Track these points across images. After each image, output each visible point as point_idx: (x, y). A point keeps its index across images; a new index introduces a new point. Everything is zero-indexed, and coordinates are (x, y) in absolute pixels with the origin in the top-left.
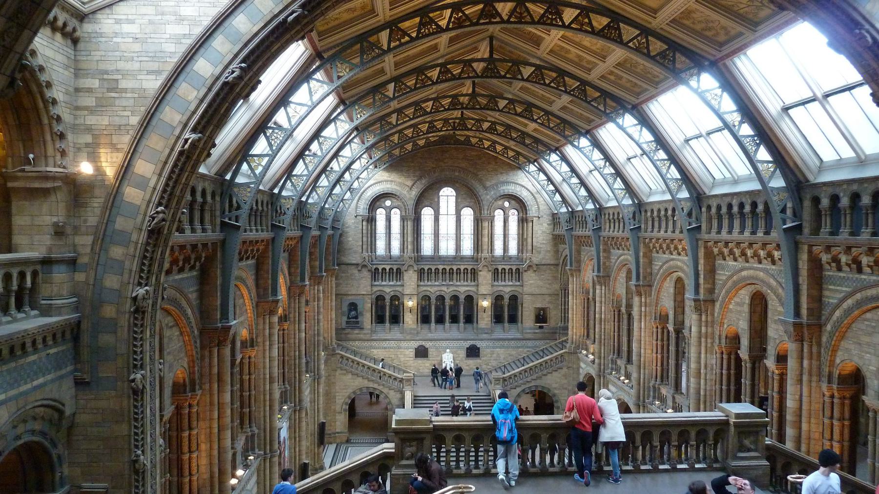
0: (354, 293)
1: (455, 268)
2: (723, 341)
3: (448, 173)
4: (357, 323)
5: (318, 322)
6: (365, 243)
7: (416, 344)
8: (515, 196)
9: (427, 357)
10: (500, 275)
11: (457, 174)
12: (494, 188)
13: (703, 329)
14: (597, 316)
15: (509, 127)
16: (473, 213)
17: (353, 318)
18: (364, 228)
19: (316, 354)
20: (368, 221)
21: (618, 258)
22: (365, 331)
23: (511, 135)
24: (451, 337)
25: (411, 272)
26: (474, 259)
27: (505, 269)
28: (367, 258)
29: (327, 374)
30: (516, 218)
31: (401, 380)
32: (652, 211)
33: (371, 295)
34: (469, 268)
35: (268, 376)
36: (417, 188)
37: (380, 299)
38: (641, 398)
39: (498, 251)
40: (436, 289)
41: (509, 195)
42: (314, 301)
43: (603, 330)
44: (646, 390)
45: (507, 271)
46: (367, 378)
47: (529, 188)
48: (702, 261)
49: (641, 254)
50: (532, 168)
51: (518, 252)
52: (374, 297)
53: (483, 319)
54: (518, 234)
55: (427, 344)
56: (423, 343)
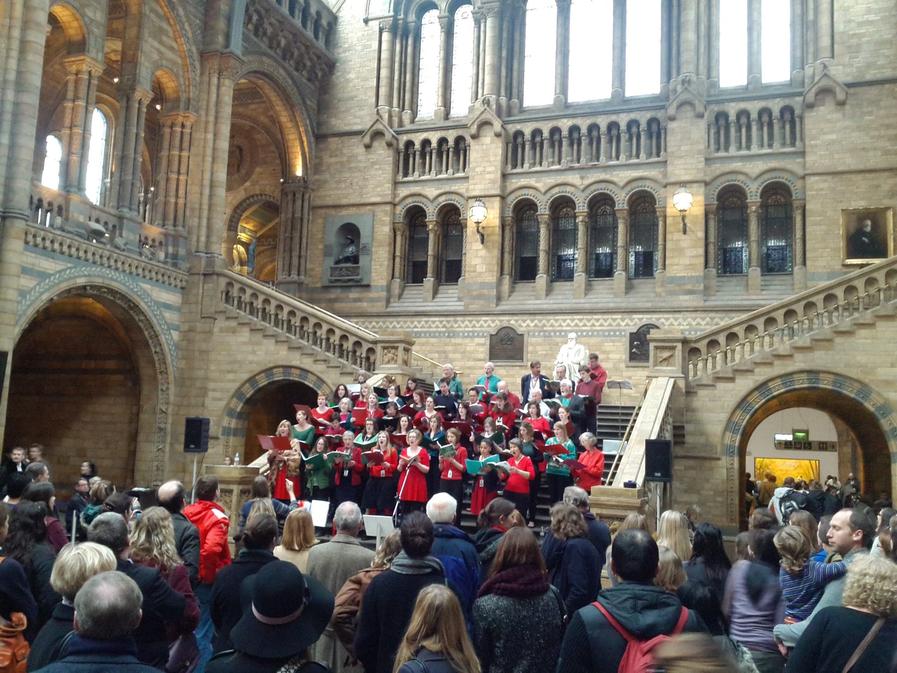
0: (352, 201)
1: (603, 122)
4: (356, 271)
5: (22, 51)
6: (384, 82)
7: (491, 325)
9: (522, 359)
10: (733, 131)
17: (347, 259)
18: (385, 46)
20: (394, 30)
22: (372, 295)
24: (587, 306)
28: (386, 116)
29: (185, 327)
34: (643, 118)
37: (415, 215)
40: (551, 180)
45: (754, 116)
46: (287, 341)
52: (400, 210)
53: (680, 251)
55: (522, 325)
56: (512, 321)
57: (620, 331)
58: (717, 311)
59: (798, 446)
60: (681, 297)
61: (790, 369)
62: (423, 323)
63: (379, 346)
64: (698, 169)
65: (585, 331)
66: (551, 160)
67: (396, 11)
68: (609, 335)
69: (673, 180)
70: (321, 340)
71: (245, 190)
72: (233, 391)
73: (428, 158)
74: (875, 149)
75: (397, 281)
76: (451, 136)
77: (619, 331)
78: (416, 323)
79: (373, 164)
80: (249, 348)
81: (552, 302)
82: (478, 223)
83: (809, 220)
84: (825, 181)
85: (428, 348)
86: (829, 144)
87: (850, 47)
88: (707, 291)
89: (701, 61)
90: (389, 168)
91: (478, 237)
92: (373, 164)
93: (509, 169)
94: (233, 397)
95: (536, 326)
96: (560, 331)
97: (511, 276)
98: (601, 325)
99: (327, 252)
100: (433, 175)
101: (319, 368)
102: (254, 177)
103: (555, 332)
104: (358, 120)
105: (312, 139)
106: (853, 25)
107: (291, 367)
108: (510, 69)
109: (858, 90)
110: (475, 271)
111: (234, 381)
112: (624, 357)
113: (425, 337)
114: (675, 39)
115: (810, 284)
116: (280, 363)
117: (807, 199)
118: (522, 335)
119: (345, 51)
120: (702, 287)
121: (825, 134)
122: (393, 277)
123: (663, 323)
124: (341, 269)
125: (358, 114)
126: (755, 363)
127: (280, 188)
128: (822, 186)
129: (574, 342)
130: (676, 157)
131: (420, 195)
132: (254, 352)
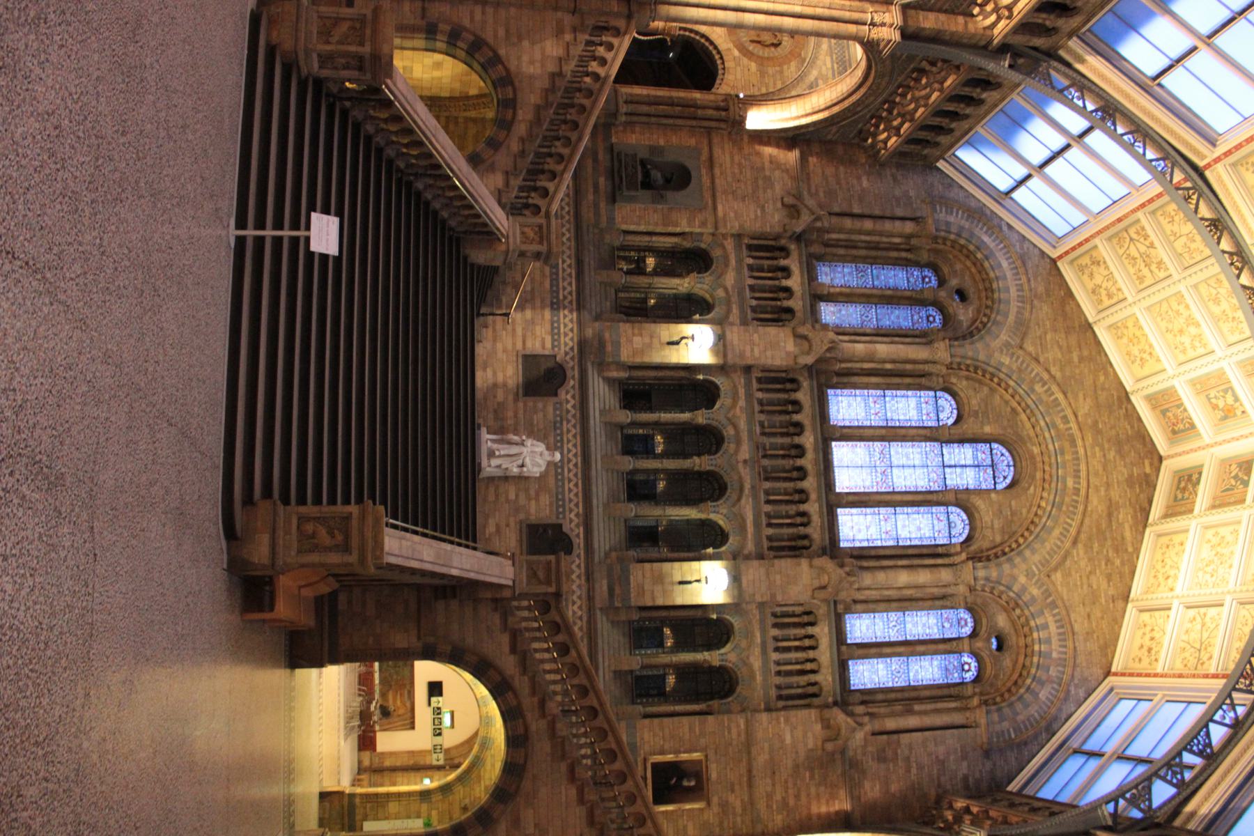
0: (717, 181)
1: (809, 484)
3: (1068, 457)
4: (632, 186)
11: (1070, 483)
12: (1047, 594)
17: (646, 174)
22: (602, 205)
24: (593, 473)
25: (790, 346)
26: (831, 547)
30: (955, 678)
36: (1020, 370)
39: (861, 628)
40: (743, 425)
55: (568, 396)
57: (564, 512)
58: (589, 622)
59: (436, 722)
60: (605, 582)
61: (529, 716)
62: (569, 270)
63: (543, 221)
64: (754, 595)
65: (563, 470)
66: (766, 424)
68: (558, 500)
69: (743, 567)
70: (550, 147)
71: (729, 49)
72: (484, 36)
73: (770, 275)
74: (774, 785)
76: (796, 303)
77: (564, 509)
78: (568, 261)
79: (763, 208)
80: (538, 56)
81: (598, 430)
82: (693, 338)
83: (696, 719)
84: (739, 735)
85: (537, 277)
86: (780, 736)
87: (884, 750)
88: (610, 609)
89: (874, 592)
90: (757, 227)
92: (763, 208)
93: (756, 374)
94: (475, 35)
95: (568, 411)
96: (562, 440)
97: (629, 378)
98: (570, 490)
99: (654, 150)
102: (745, 60)
103: (561, 435)
105: (790, 134)
106: (907, 752)
107: (515, 109)
108: (870, 373)
110: (634, 335)
111: (496, 36)
112: (533, 518)
113: (551, 274)
114: (901, 563)
115: (623, 724)
116: (519, 95)
117: (720, 717)
118: (556, 395)
119: (892, 175)
120: (617, 604)
121: (792, 731)
123: (574, 561)
124: (634, 167)
126: (534, 676)
127: (732, 93)
128: (734, 731)
129: (549, 458)
130: (767, 570)
131: (727, 265)
132: (532, 62)
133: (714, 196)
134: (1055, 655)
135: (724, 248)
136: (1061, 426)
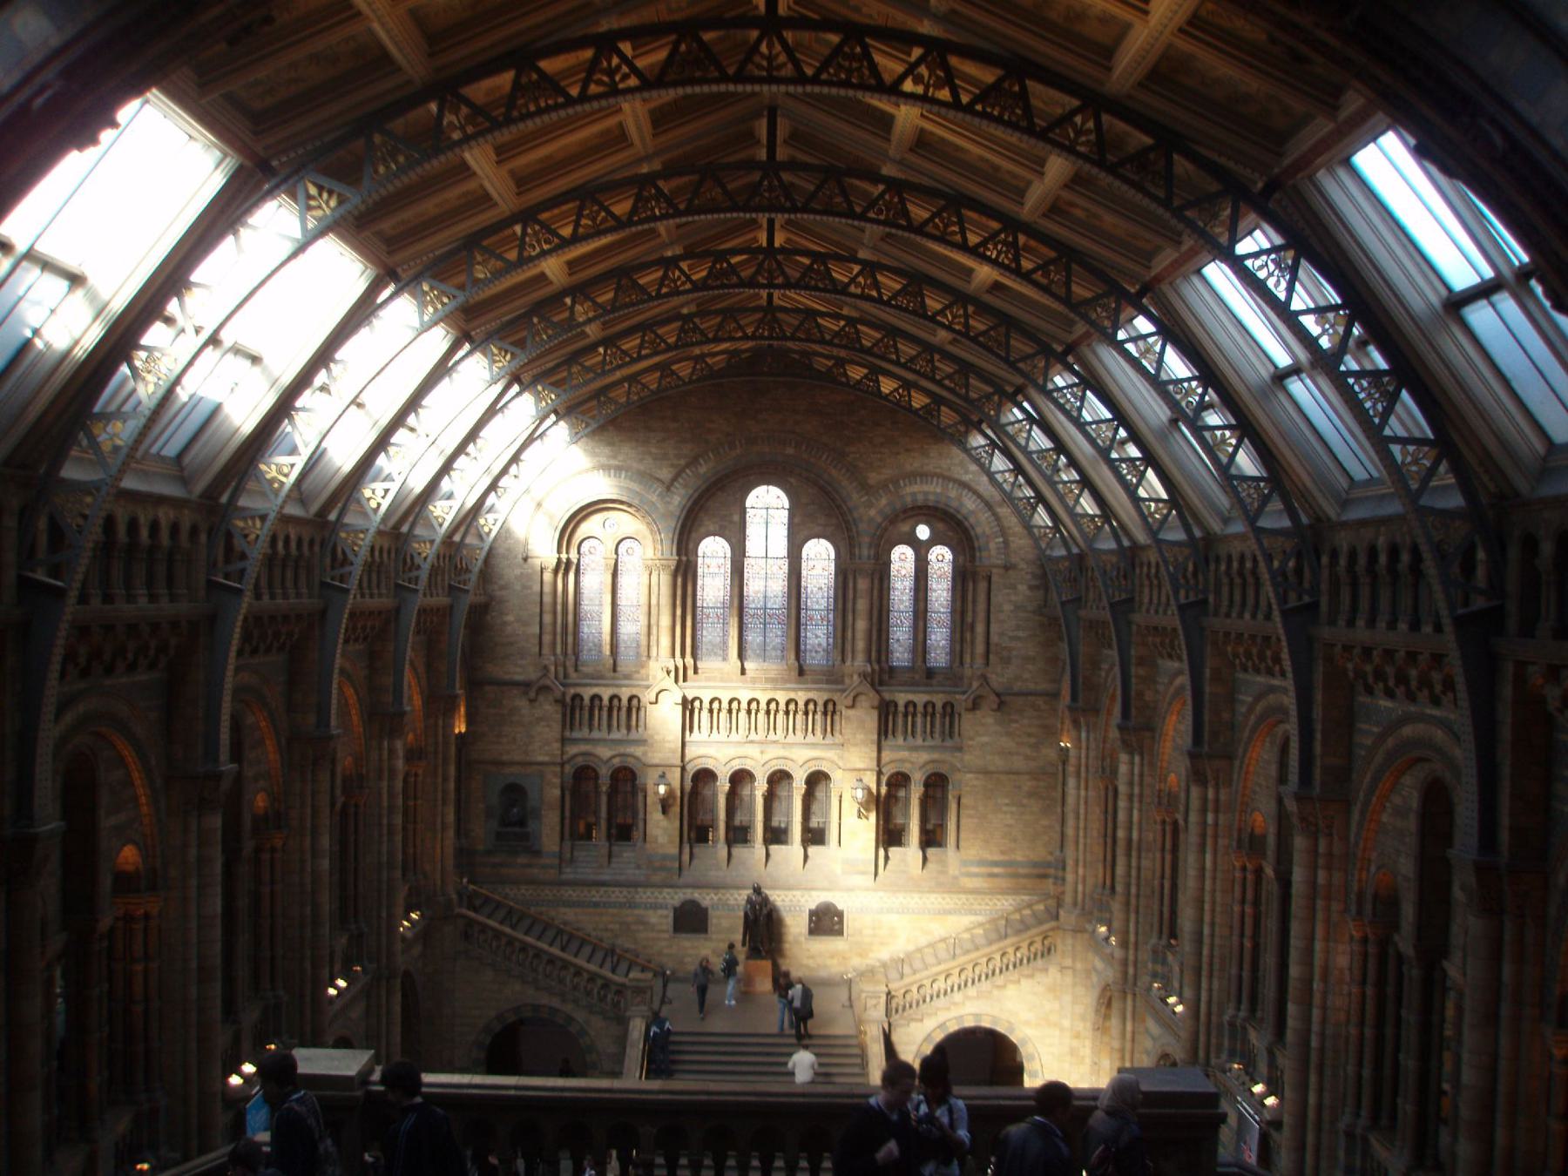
0: (517, 757)
2: (1368, 908)
7: (676, 897)
8: (945, 513)
13: (1322, 876)
14: (1121, 834)
15: (894, 332)
16: (833, 556)
19: (384, 914)
21: (1171, 683)
23: (897, 351)
27: (915, 705)
28: (553, 668)
31: (621, 990)
32: (1230, 559)
33: (562, 765)
35: (194, 964)
36: (685, 486)
38: (1201, 1054)
40: (732, 752)
41: (929, 507)
42: (380, 778)
43: (1134, 873)
44: (1214, 1033)
45: (920, 708)
47: (981, 489)
48: (1319, 697)
49: (1208, 673)
50: (977, 441)
51: (952, 661)
52: (568, 769)
54: (953, 612)
56: (696, 895)
67: (559, 552)
69: (849, 766)
73: (597, 712)
75: (568, 844)
78: (594, 893)
79: (540, 719)
90: (557, 727)
91: (660, 808)
92: (540, 719)
95: (720, 899)
100: (604, 734)
101: (568, 1008)
104: (518, 670)
109: (1008, 699)
110: (656, 841)
122: (562, 839)
125: (520, 662)
128: (975, 783)
133: (531, 764)
134: (939, 490)
135: (575, 756)
136: (738, 451)
